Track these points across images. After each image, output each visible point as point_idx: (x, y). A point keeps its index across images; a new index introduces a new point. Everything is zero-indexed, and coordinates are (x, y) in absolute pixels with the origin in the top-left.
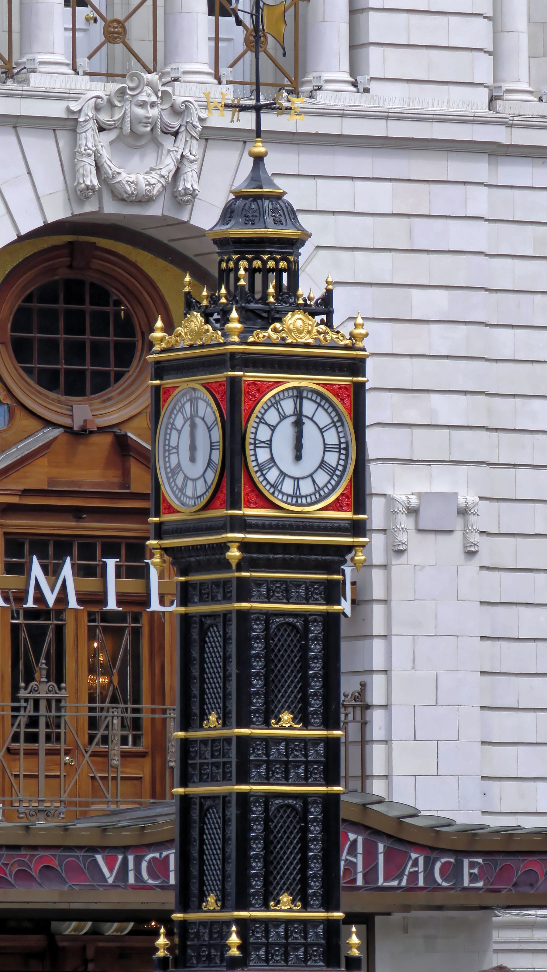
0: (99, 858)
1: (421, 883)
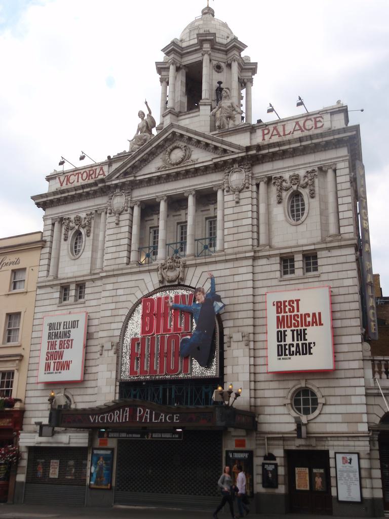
0: (90, 416)
1: (163, 421)
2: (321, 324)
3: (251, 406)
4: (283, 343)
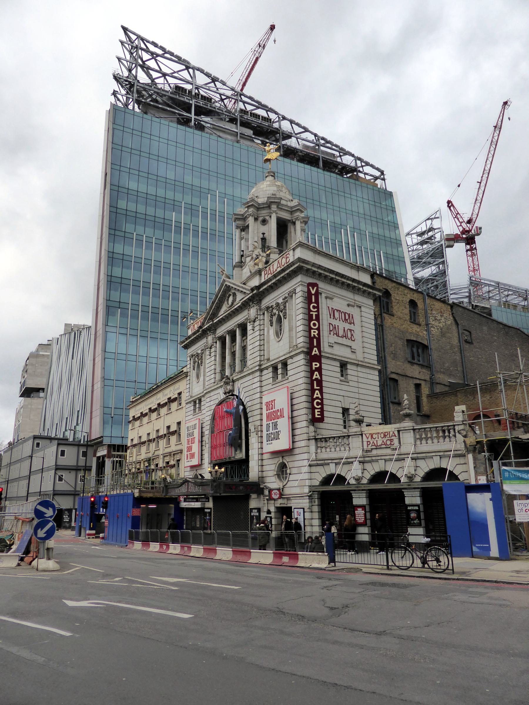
2: (284, 417)
3: (259, 477)
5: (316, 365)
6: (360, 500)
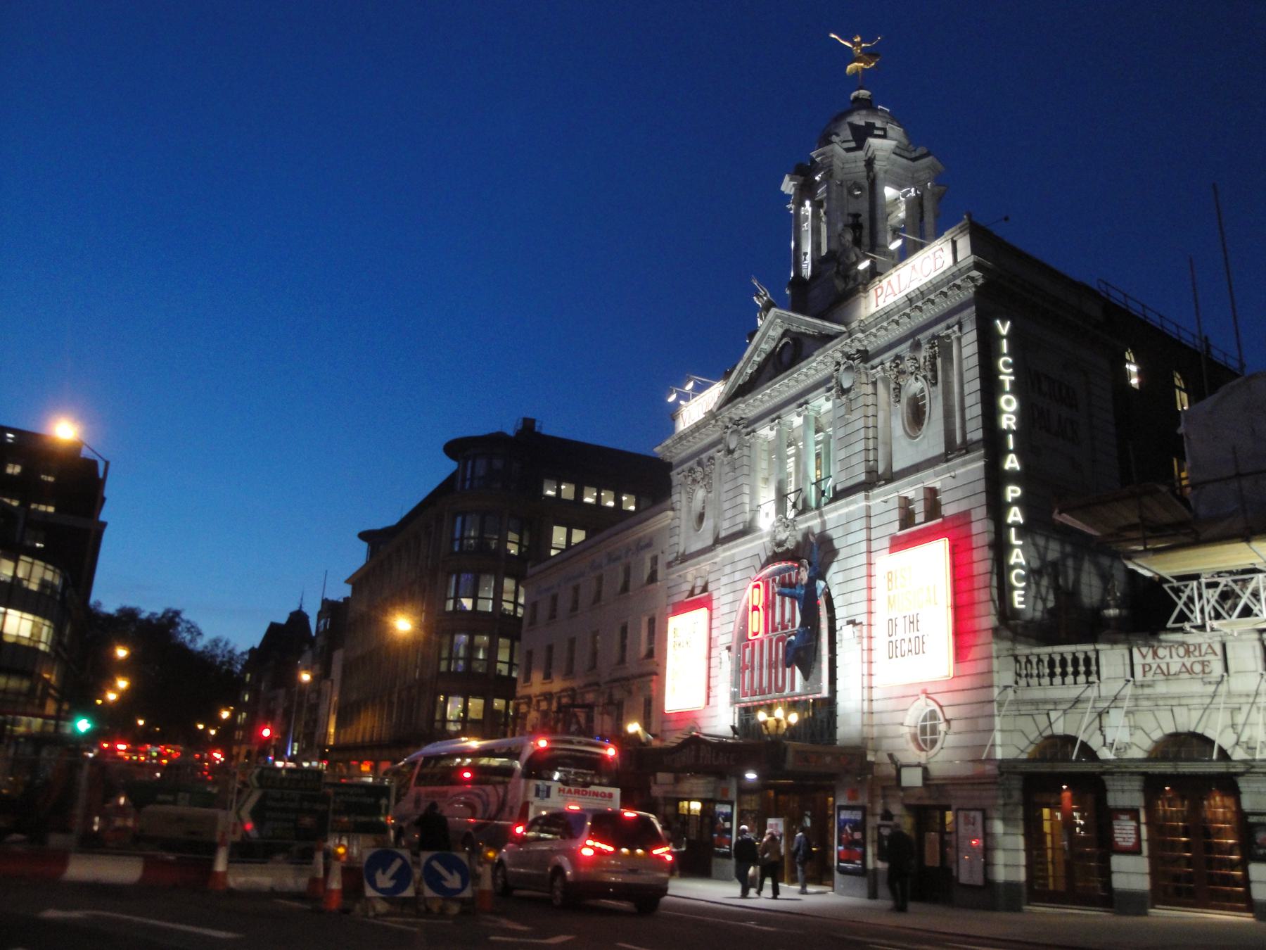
4: (892, 639)
5: (1014, 491)
6: (1125, 795)
